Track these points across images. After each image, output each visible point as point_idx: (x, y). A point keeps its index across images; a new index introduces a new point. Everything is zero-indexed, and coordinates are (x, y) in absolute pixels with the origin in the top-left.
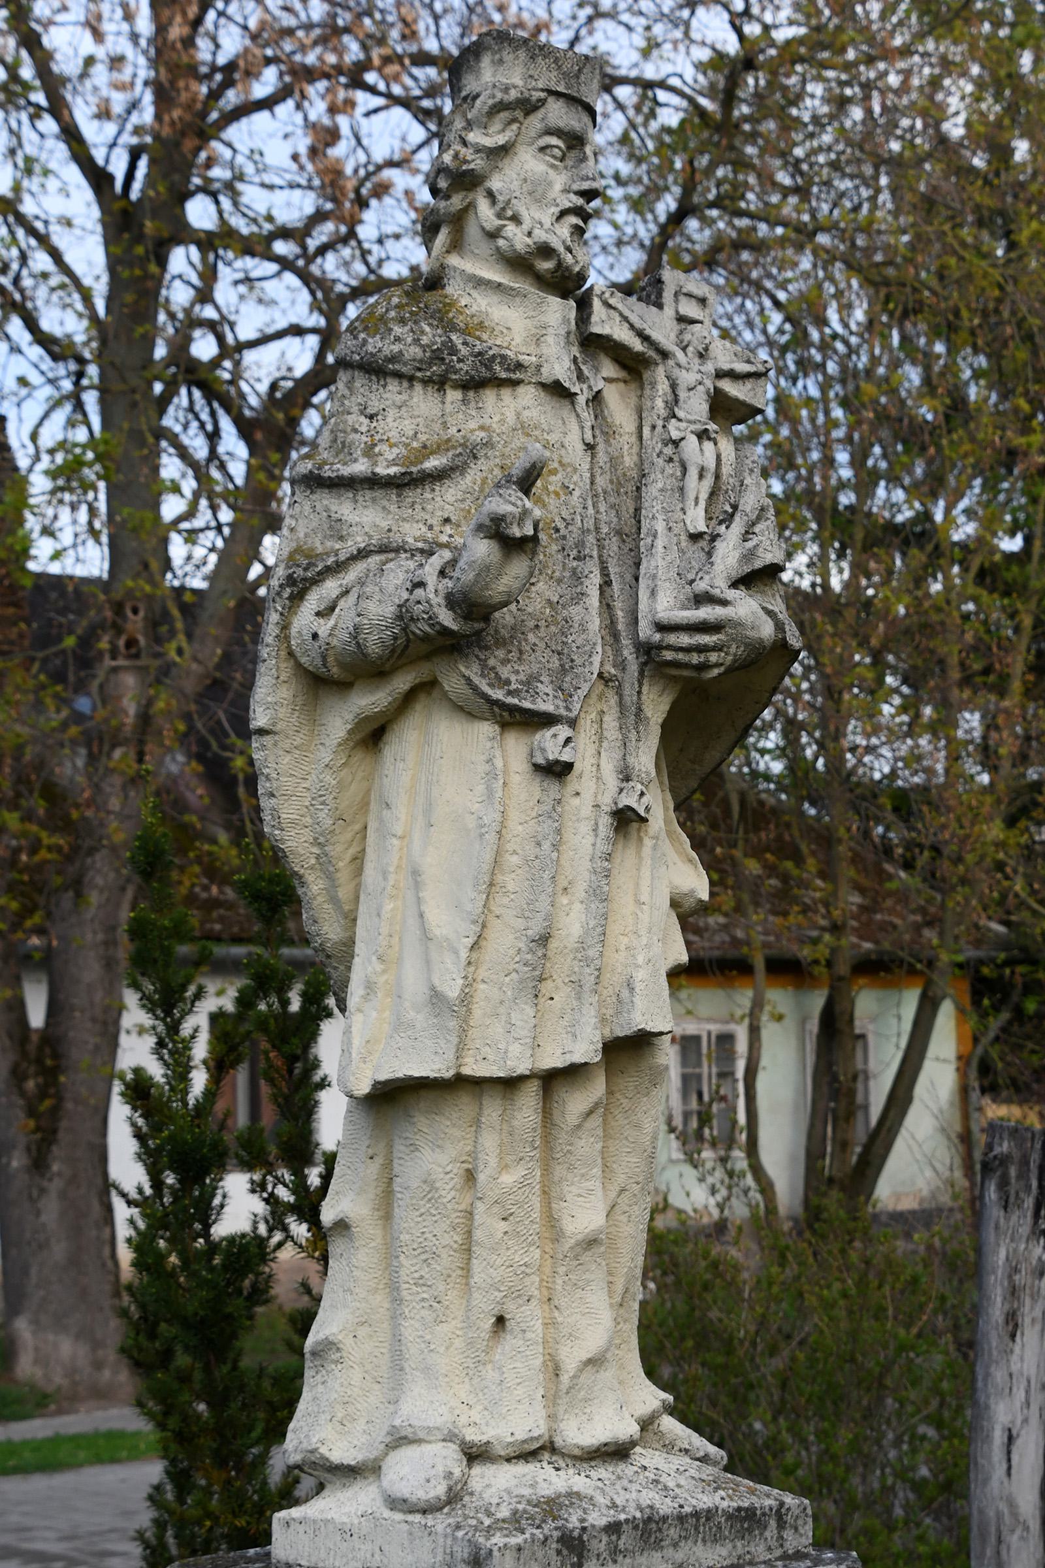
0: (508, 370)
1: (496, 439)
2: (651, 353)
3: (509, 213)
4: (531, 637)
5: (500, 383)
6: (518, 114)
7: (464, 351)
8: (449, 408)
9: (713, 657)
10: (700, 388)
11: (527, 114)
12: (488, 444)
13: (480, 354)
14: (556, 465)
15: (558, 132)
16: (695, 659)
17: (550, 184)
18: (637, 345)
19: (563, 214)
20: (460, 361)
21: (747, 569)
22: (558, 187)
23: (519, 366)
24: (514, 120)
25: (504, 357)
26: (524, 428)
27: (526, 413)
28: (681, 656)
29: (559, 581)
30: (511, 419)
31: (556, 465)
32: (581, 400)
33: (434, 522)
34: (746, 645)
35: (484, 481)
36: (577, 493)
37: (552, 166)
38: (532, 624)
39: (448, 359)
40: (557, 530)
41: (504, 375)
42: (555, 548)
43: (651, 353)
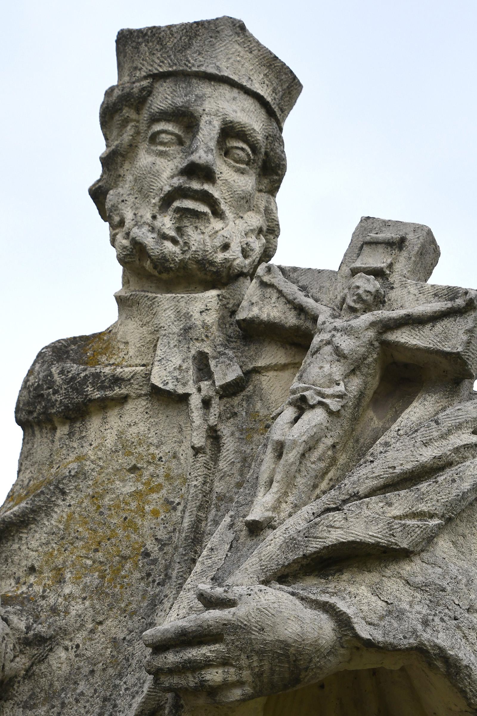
0: (102, 388)
1: (88, 466)
2: (309, 324)
3: (117, 219)
4: (82, 687)
5: (105, 405)
6: (127, 112)
7: (58, 379)
8: (57, 444)
9: (215, 676)
10: (328, 349)
11: (138, 110)
12: (80, 474)
13: (73, 378)
14: (161, 480)
15: (164, 116)
16: (191, 681)
17: (157, 175)
18: (291, 319)
19: (166, 201)
20: (56, 392)
21: (292, 557)
22: (166, 174)
23: (117, 380)
24: (126, 122)
25: (97, 376)
26: (124, 446)
27: (134, 430)
28: (175, 680)
29: (133, 613)
30: (111, 440)
31: (161, 480)
32: (195, 401)
33: (20, 573)
34: (261, 653)
35: (70, 517)
36: (180, 508)
37: (161, 154)
38: (85, 670)
39: (45, 392)
40: (147, 554)
41: (97, 395)
42: (137, 575)
43: (309, 324)
